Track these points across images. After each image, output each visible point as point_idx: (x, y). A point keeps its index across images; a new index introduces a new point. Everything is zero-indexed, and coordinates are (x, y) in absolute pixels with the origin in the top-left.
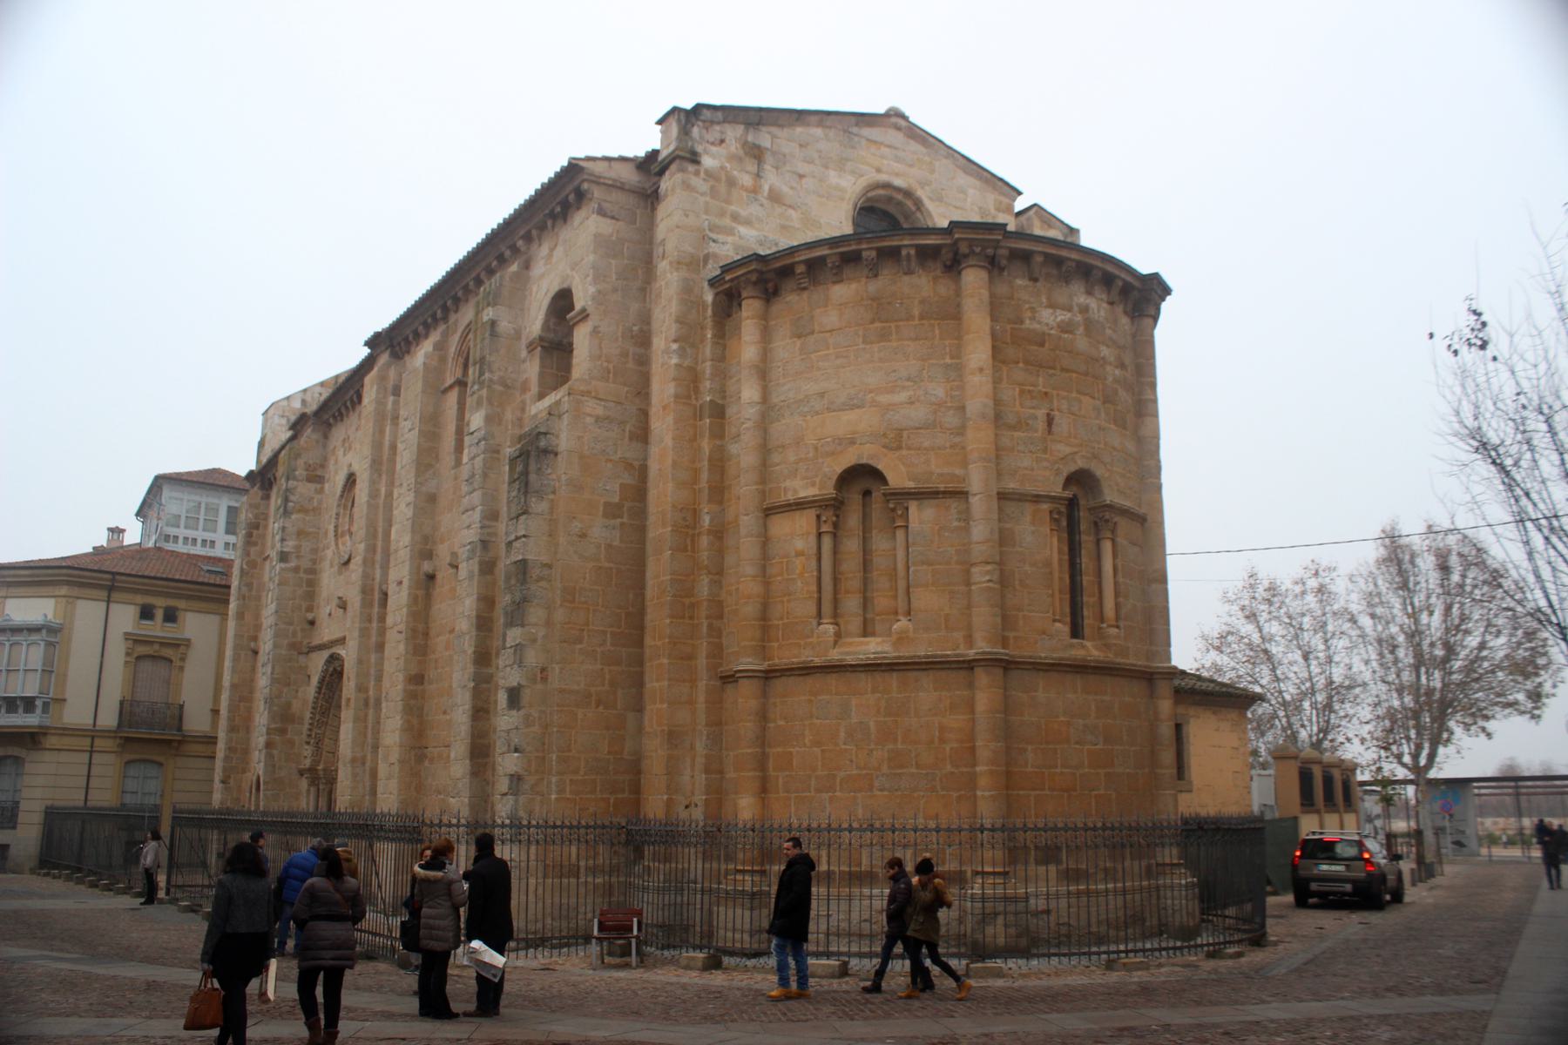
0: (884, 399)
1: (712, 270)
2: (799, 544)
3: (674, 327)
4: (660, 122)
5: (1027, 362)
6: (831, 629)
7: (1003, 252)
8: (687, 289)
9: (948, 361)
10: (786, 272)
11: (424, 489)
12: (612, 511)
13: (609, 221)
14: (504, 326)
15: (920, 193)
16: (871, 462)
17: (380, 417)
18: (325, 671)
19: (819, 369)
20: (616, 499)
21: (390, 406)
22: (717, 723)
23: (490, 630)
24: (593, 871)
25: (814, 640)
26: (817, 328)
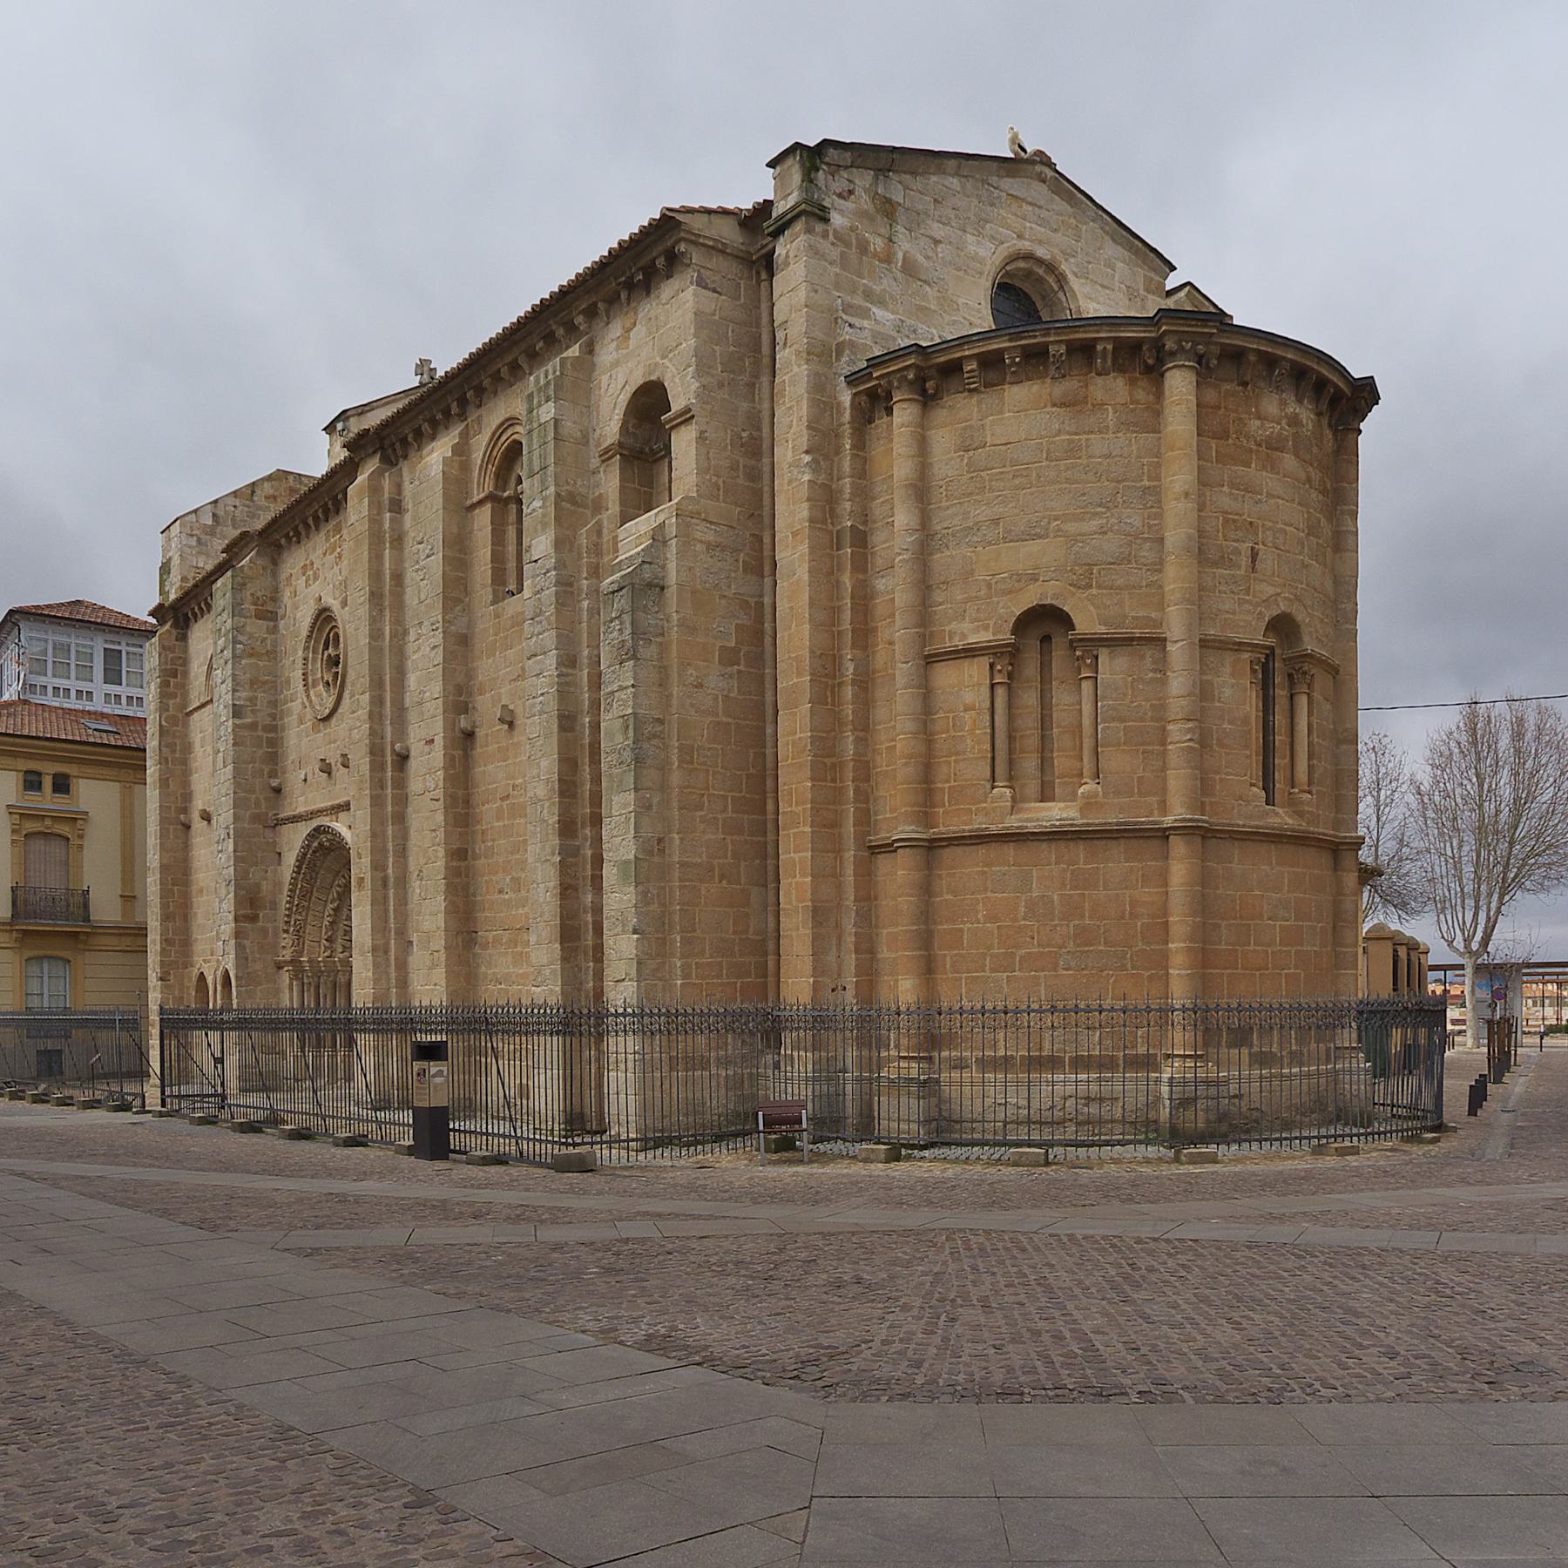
0: (1071, 527)
1: (845, 366)
2: (969, 697)
5: (1232, 486)
7: (1215, 350)
8: (820, 389)
17: (376, 538)
19: (991, 490)
22: (868, 895)
23: (574, 796)
24: (725, 1062)
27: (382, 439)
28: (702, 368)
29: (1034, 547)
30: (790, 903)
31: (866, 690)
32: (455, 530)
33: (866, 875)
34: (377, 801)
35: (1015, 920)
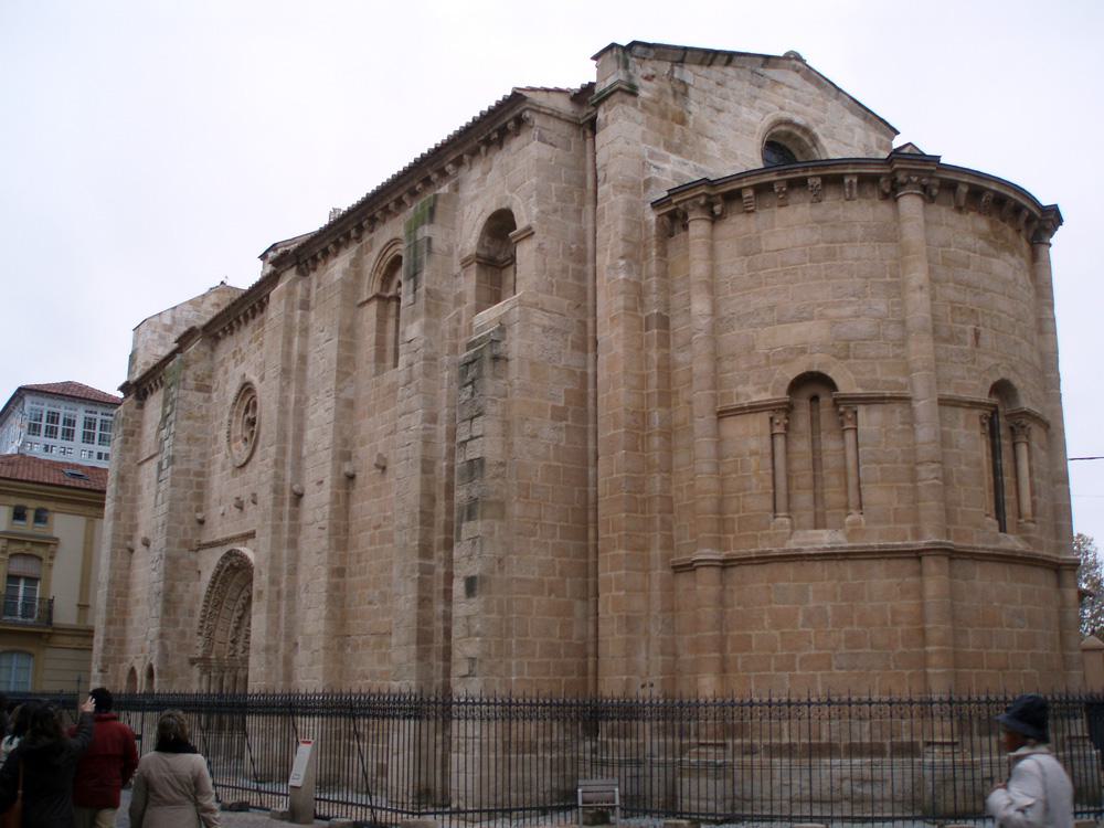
0: (832, 312)
2: (753, 444)
3: (621, 245)
4: (595, 58)
5: (958, 282)
7: (936, 182)
8: (631, 210)
9: (888, 279)
10: (733, 197)
11: (342, 395)
12: (558, 414)
13: (548, 147)
14: (437, 243)
15: (816, 130)
16: (823, 370)
18: (220, 567)
19: (766, 284)
20: (562, 404)
23: (431, 525)
24: (551, 747)
25: (771, 532)
26: (764, 248)
28: (542, 197)
29: (802, 327)
30: (607, 612)
31: (669, 440)
32: (348, 321)
33: (669, 590)
34: (276, 530)
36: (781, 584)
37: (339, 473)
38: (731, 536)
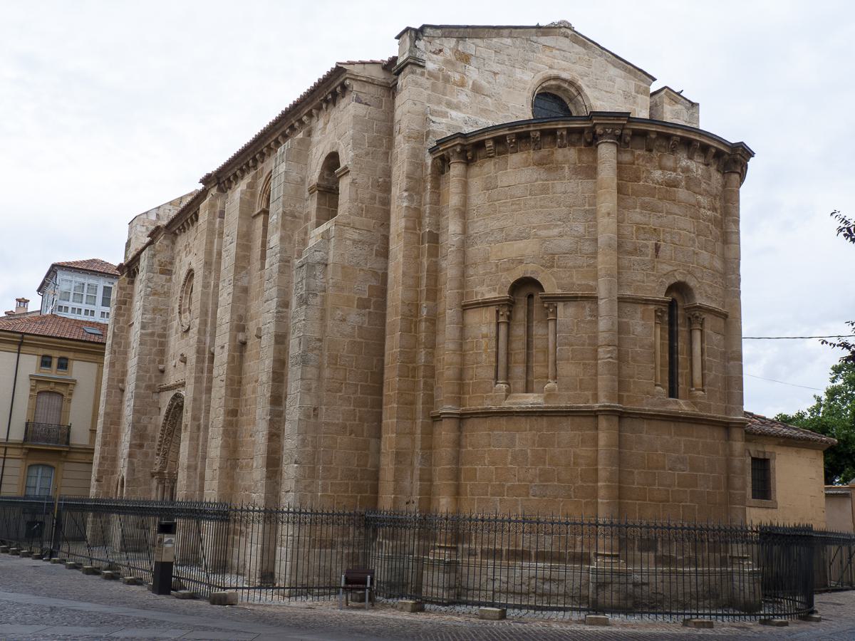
0: (543, 233)
2: (485, 330)
4: (398, 37)
6: (504, 386)
12: (363, 304)
13: (363, 106)
15: (580, 83)
16: (532, 276)
17: (211, 232)
18: (171, 405)
19: (500, 212)
20: (366, 297)
21: (217, 226)
22: (429, 448)
26: (499, 184)
27: (219, 179)
28: (356, 143)
29: (521, 244)
31: (434, 324)
32: (245, 229)
33: (428, 434)
35: (506, 464)
36: (496, 432)
37: (235, 341)
38: (468, 396)
